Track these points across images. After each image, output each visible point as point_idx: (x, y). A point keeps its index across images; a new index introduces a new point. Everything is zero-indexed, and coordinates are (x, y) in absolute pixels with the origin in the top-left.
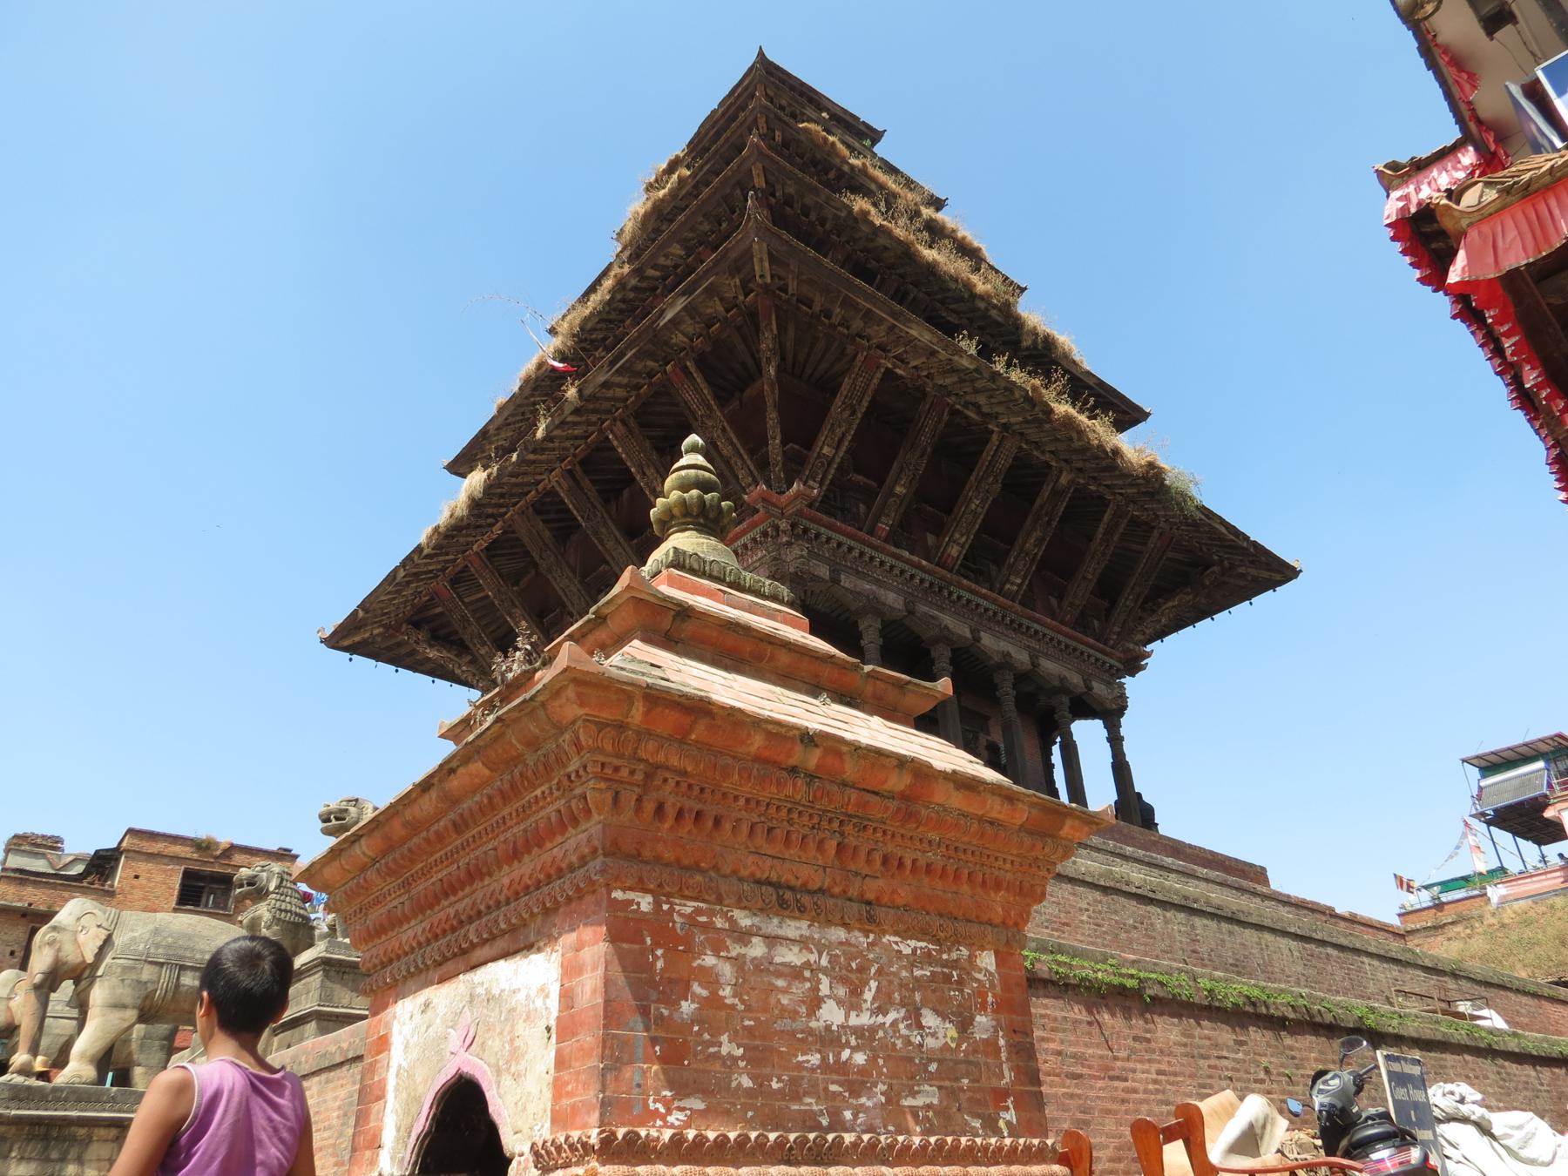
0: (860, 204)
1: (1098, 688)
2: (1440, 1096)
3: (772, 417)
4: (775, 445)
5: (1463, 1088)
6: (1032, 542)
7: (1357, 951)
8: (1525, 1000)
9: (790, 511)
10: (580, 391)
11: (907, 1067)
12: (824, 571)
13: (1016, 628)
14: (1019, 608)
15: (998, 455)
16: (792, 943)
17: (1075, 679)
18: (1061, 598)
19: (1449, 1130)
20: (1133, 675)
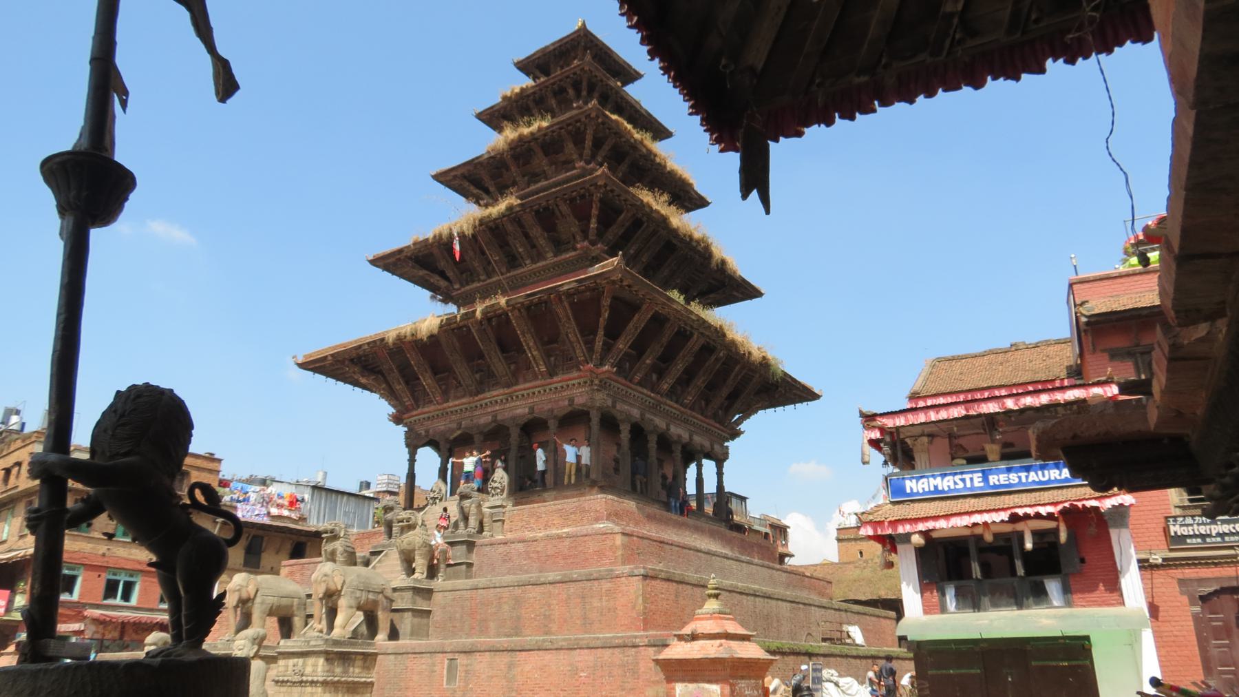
0: (646, 196)
1: (717, 447)
2: (826, 673)
3: (601, 333)
5: (833, 672)
6: (700, 381)
8: (874, 619)
9: (602, 376)
10: (507, 302)
12: (609, 402)
13: (686, 422)
14: (689, 412)
15: (695, 343)
16: (743, 684)
17: (707, 444)
18: (707, 405)
19: (826, 685)
20: (733, 439)
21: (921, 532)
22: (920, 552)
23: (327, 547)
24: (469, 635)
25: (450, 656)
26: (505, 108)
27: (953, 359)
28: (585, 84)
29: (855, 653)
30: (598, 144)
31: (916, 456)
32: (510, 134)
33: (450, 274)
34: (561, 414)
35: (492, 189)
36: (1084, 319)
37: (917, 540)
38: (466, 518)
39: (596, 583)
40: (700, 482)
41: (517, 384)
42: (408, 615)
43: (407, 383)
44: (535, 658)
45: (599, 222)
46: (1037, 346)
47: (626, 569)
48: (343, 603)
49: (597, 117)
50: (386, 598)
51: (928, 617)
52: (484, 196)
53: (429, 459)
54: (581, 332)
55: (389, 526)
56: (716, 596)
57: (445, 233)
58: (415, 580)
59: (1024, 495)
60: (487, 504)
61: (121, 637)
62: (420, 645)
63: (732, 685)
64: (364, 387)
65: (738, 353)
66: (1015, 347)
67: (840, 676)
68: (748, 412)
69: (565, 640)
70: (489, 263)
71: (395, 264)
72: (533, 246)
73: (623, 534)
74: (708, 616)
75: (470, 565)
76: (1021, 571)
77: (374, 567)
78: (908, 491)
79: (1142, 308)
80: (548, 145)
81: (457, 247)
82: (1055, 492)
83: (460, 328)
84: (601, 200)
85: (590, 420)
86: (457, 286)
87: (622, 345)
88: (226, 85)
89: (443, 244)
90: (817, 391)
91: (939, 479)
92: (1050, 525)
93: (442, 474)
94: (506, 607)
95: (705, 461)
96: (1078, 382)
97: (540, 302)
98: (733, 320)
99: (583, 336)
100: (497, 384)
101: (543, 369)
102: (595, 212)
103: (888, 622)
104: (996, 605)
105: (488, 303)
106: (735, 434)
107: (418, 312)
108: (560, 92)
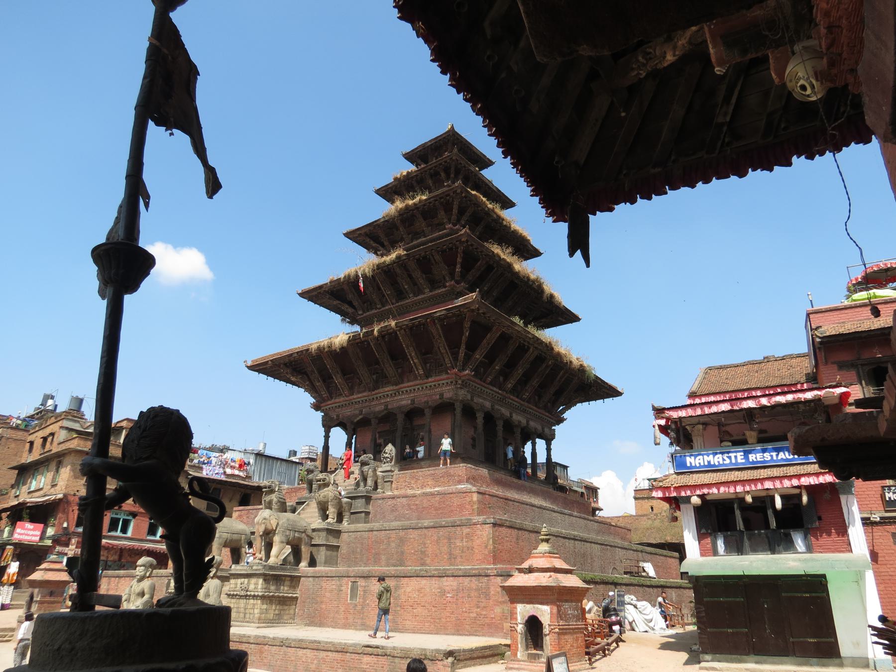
0: (496, 249)
1: (546, 430)
2: (627, 598)
3: (463, 347)
4: (462, 355)
5: (633, 597)
6: (535, 382)
7: (615, 547)
8: (662, 557)
9: (463, 378)
10: (396, 324)
11: (574, 616)
12: (469, 397)
13: (524, 411)
14: (526, 404)
15: (531, 355)
16: (566, 605)
17: (539, 428)
19: (627, 606)
21: (698, 496)
22: (697, 510)
23: (266, 498)
24: (366, 565)
25: (353, 579)
26: (396, 186)
27: (721, 368)
28: (453, 169)
29: (648, 583)
30: (461, 212)
31: (694, 439)
32: (399, 204)
33: (356, 304)
34: (435, 404)
35: (386, 243)
36: (818, 340)
37: (696, 500)
38: (365, 479)
39: (459, 528)
40: (534, 455)
41: (402, 382)
42: (323, 549)
43: (324, 381)
44: (414, 583)
45: (462, 267)
46: (783, 359)
47: (481, 519)
48: (277, 539)
49: (462, 192)
50: (308, 536)
51: (703, 558)
52: (380, 248)
53: (339, 436)
54: (449, 346)
55: (310, 483)
56: (547, 541)
57: (353, 274)
58: (329, 523)
59: (775, 469)
60: (380, 469)
61: (120, 560)
62: (331, 571)
63: (558, 607)
64: (293, 384)
65: (562, 362)
66: (767, 360)
67: (638, 600)
68: (569, 405)
69: (436, 570)
70: (384, 296)
71: (316, 296)
72: (415, 284)
73: (478, 493)
74: (542, 556)
75: (367, 513)
76: (773, 524)
77: (299, 514)
78: (688, 465)
79: (862, 332)
80: (425, 212)
81: (362, 285)
82: (798, 467)
83: (362, 342)
84: (464, 252)
85: (455, 409)
86: (360, 312)
87: (478, 356)
88: (213, 185)
89: (351, 282)
90: (619, 389)
91: (711, 456)
92: (797, 491)
93: (349, 445)
94: (393, 545)
95: (537, 440)
96: (815, 386)
97: (420, 324)
98: (560, 338)
99: (450, 349)
100: (389, 383)
101: (421, 372)
102: (459, 260)
103: (673, 560)
104: (755, 550)
105: (382, 325)
106: (560, 421)
107: (331, 330)
108: (435, 175)
